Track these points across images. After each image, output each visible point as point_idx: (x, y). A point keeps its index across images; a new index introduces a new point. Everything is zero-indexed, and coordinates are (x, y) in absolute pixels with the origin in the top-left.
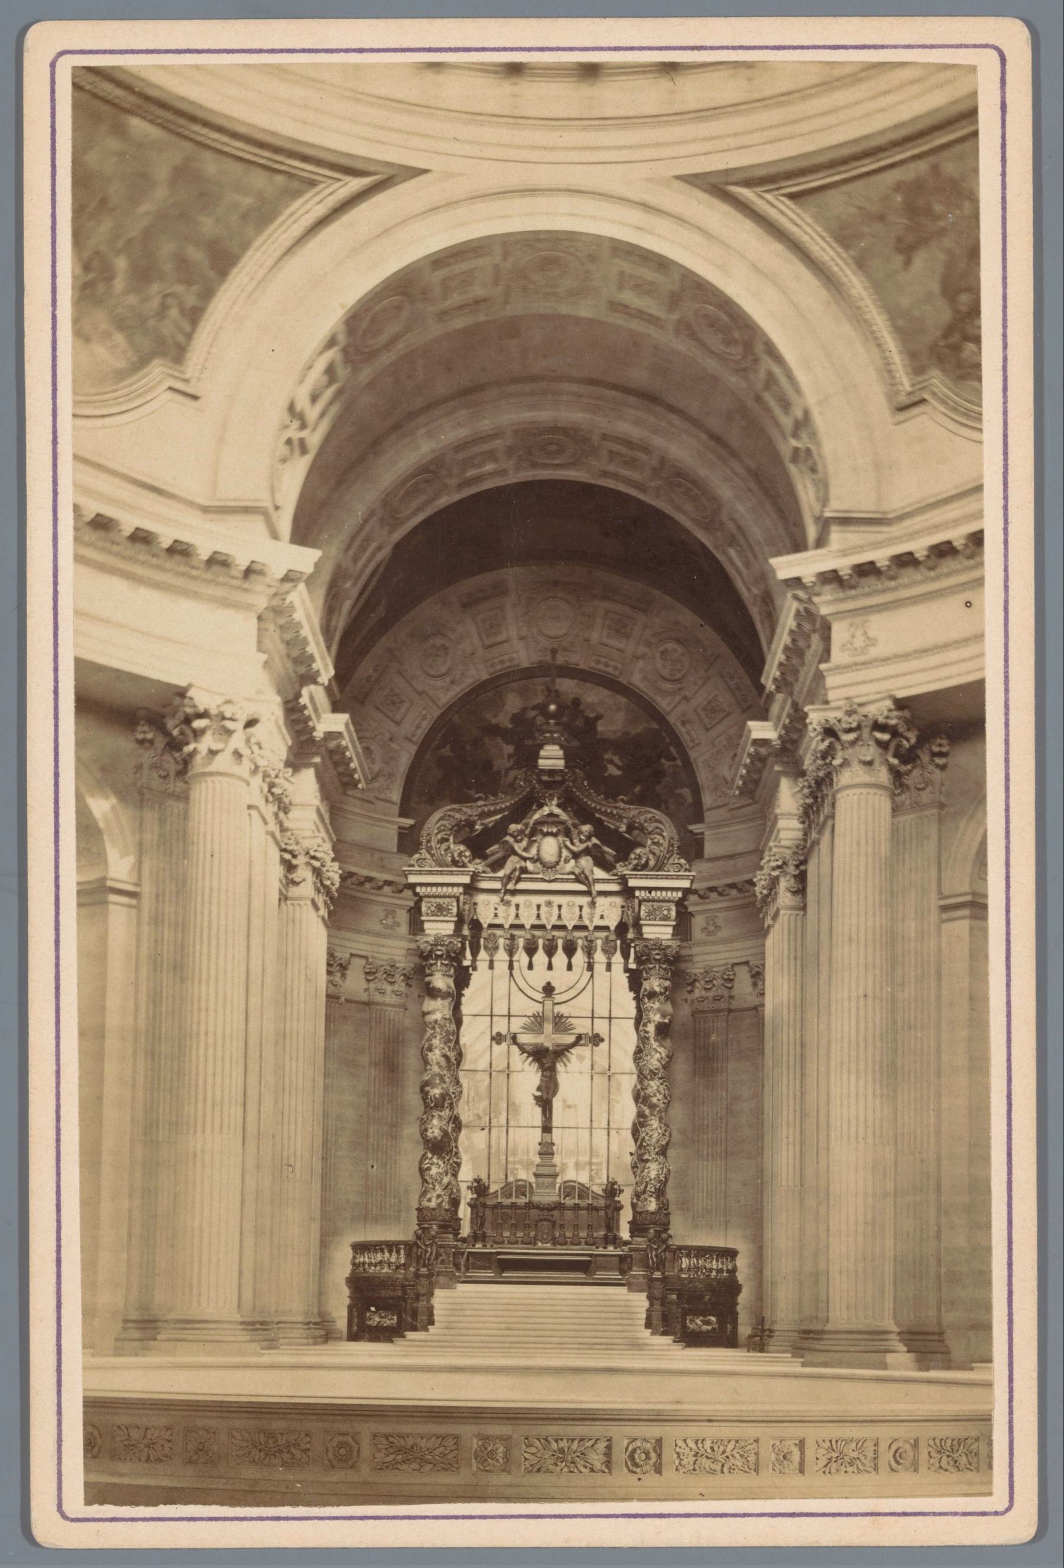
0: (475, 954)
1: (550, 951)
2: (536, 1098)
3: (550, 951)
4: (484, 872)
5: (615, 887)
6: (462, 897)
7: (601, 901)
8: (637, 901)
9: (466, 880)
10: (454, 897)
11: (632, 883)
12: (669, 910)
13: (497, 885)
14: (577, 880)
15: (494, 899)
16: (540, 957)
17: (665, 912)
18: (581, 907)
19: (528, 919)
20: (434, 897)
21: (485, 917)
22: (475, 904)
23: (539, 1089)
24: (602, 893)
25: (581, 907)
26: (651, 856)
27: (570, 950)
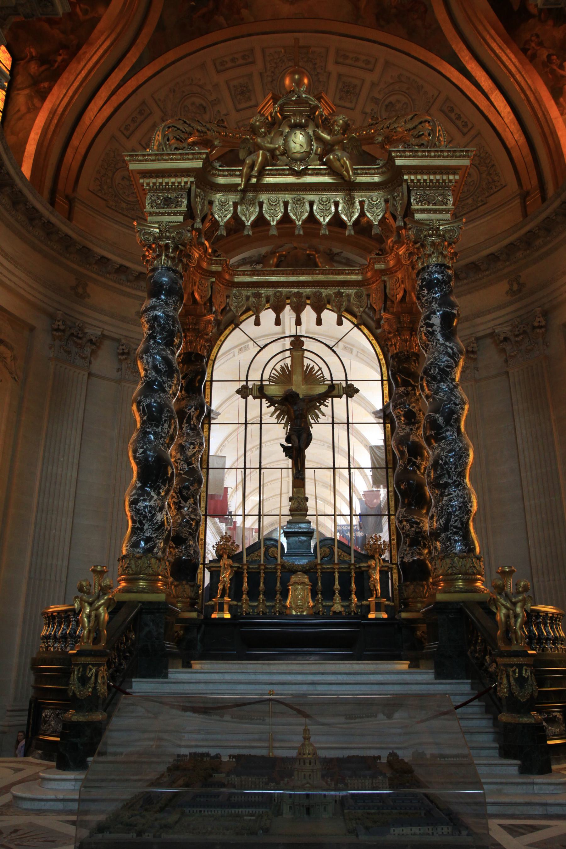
2: (286, 450)
5: (376, 179)
6: (194, 187)
8: (405, 186)
9: (198, 164)
11: (399, 162)
12: (444, 196)
13: (238, 180)
14: (332, 171)
15: (232, 198)
16: (288, 314)
17: (440, 198)
18: (336, 204)
22: (211, 203)
23: (288, 440)
25: (336, 204)
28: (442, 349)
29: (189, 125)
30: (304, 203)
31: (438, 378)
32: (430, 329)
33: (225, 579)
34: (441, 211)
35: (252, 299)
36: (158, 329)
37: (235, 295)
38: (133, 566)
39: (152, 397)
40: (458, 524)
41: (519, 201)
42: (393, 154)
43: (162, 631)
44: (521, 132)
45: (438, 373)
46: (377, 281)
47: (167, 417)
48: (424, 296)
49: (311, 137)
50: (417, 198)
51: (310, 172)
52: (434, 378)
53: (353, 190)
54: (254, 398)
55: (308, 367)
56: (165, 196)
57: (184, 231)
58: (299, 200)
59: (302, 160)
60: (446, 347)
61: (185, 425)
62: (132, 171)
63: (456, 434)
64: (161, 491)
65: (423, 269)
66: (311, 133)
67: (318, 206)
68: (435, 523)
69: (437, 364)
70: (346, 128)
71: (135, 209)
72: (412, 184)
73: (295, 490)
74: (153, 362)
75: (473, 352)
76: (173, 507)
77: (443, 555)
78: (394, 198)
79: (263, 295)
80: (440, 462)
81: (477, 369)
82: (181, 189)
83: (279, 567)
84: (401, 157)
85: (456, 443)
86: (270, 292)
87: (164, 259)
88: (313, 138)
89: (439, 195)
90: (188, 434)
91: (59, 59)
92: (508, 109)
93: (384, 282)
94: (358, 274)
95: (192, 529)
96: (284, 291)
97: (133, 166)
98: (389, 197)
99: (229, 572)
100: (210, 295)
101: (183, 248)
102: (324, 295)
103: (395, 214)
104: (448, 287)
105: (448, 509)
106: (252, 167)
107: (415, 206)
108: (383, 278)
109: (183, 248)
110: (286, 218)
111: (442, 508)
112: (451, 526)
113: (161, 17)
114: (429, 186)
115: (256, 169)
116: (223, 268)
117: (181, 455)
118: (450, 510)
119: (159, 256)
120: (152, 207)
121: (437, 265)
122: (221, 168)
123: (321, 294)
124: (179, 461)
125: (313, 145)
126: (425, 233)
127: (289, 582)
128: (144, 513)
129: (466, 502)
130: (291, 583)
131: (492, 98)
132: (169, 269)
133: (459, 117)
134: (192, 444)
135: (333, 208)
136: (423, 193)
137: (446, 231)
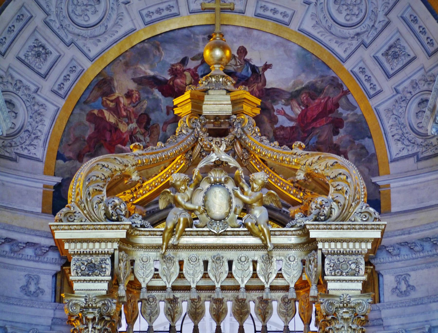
0: (131, 321)
1: (218, 316)
3: (218, 316)
4: (142, 226)
5: (293, 240)
6: (117, 253)
7: (276, 254)
9: (122, 234)
10: (108, 253)
11: (313, 234)
13: (158, 240)
14: (251, 233)
15: (153, 254)
18: (255, 263)
19: (194, 277)
20: (85, 254)
21: (144, 278)
22: (132, 262)
24: (277, 247)
25: (255, 263)
26: (334, 205)
27: (241, 313)
30: (223, 262)
42: (308, 227)
46: (305, 287)
49: (230, 193)
50: (330, 266)
51: (229, 233)
56: (89, 262)
57: (110, 304)
58: (219, 259)
59: (220, 220)
62: (57, 239)
67: (236, 266)
71: (13, 144)
79: (179, 300)
87: (92, 331)
88: (233, 197)
96: (204, 295)
97: (59, 235)
98: (305, 259)
119: (87, 328)
120: (77, 273)
122: (142, 229)
126: (337, 305)
133: (424, 33)
135: (251, 268)
136: (336, 260)
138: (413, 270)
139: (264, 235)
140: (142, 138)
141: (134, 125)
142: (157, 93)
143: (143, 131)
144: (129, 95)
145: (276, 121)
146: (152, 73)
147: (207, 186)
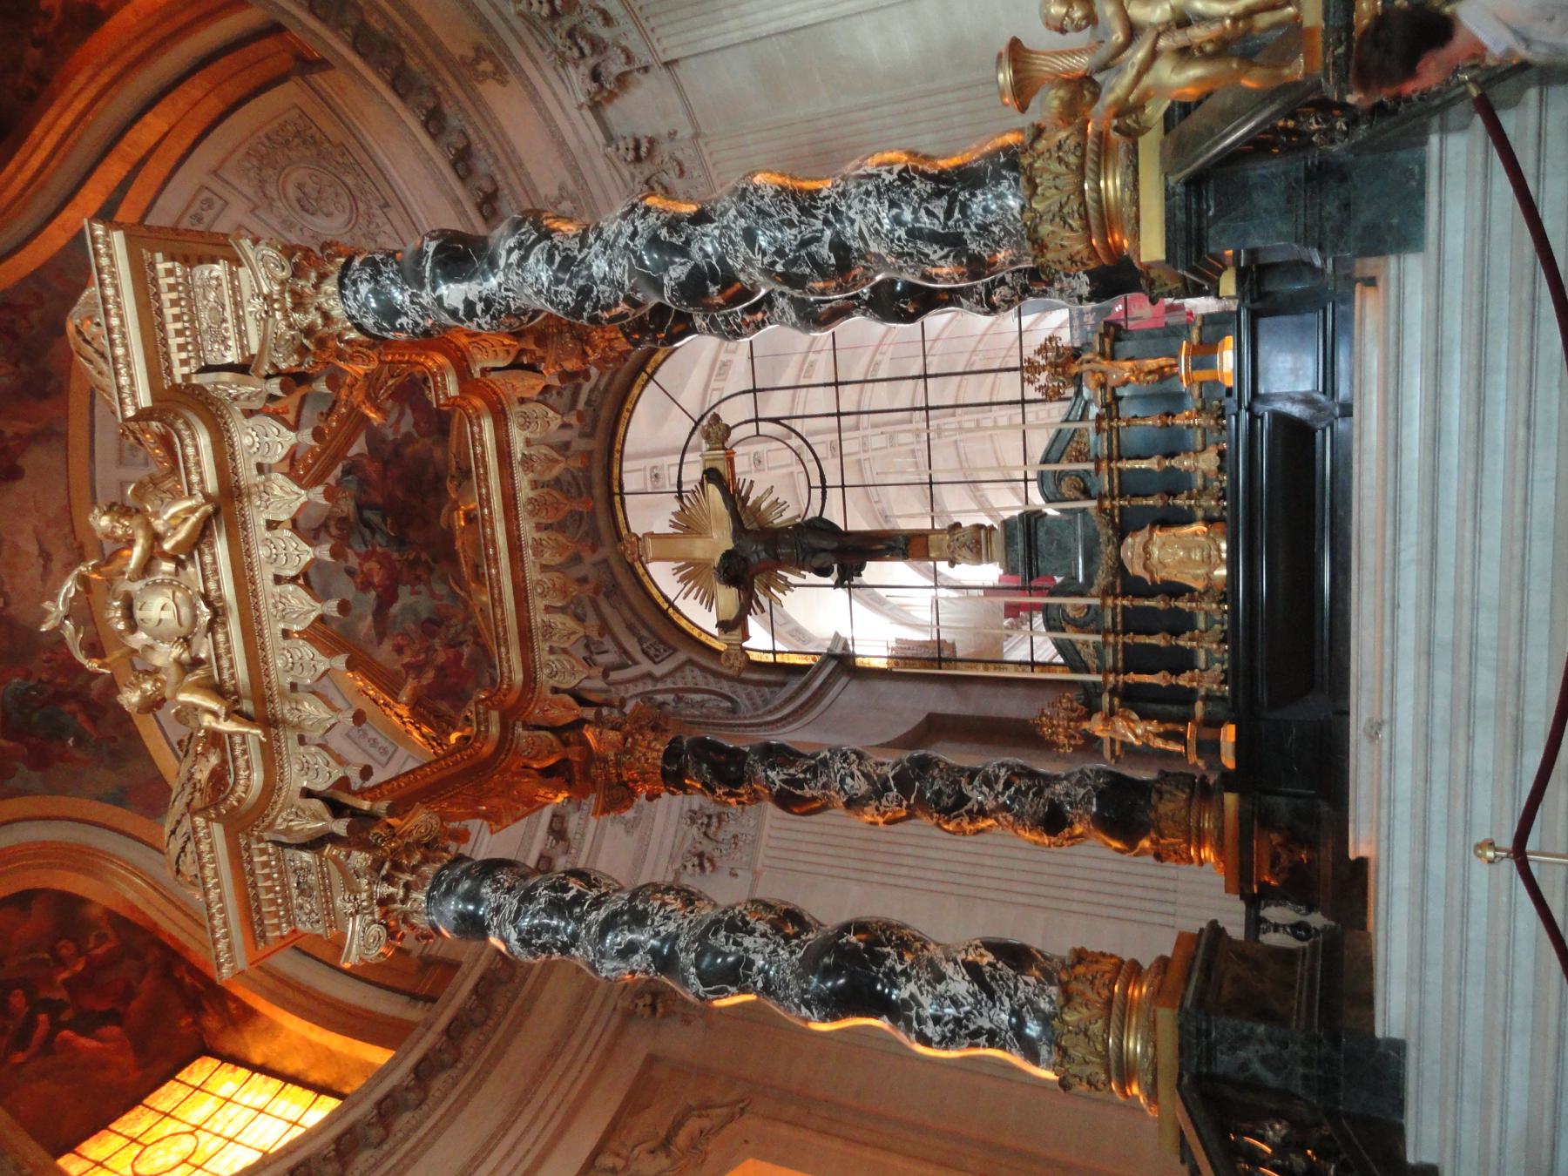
5: (204, 439)
11: (145, 400)
12: (206, 286)
17: (212, 296)
22: (307, 793)
23: (823, 572)
28: (515, 278)
29: (179, 822)
31: (581, 282)
32: (480, 307)
33: (1139, 731)
34: (236, 290)
35: (556, 642)
36: (545, 937)
37: (552, 676)
38: (1089, 1070)
39: (684, 970)
40: (938, 207)
41: (316, 76)
42: (130, 413)
43: (1261, 1029)
44: (185, 87)
45: (569, 284)
47: (728, 938)
48: (417, 324)
51: (212, 585)
52: (585, 292)
53: (238, 488)
54: (746, 637)
55: (675, 525)
59: (194, 607)
60: (509, 266)
61: (808, 792)
63: (709, 228)
64: (899, 968)
65: (359, 327)
66: (137, 586)
68: (945, 270)
69: (549, 289)
70: (120, 510)
72: (193, 361)
73: (932, 555)
74: (613, 959)
75: (637, 147)
76: (982, 824)
77: (1027, 244)
78: (235, 399)
80: (779, 268)
81: (672, 135)
82: (278, 859)
83: (1109, 601)
84: (133, 395)
85: (728, 227)
86: (537, 604)
88: (150, 580)
89: (205, 297)
90: (825, 786)
91: (188, 980)
92: (149, 117)
93: (484, 371)
94: (480, 426)
95: (1029, 788)
99: (1120, 724)
100: (549, 735)
101: (387, 865)
102: (531, 494)
103: (264, 396)
104: (385, 265)
105: (899, 239)
106: (215, 714)
107: (231, 357)
108: (477, 375)
109: (387, 865)
110: (309, 635)
111: (900, 255)
112: (945, 226)
113: (98, 799)
114: (191, 321)
115: (214, 706)
116: (494, 708)
117: (867, 805)
118: (901, 232)
121: (343, 297)
123: (530, 501)
124: (882, 809)
125: (162, 583)
126: (282, 325)
127: (1140, 580)
128: (951, 1026)
129: (877, 187)
130: (1147, 577)
131: (138, 154)
132: (429, 898)
134: (842, 781)
137: (271, 278)
138: (535, 190)
139: (192, 510)
140: (453, 630)
141: (437, 642)
142: (395, 609)
143: (443, 629)
144: (399, 650)
145: (408, 435)
146: (370, 618)
147: (141, 637)
